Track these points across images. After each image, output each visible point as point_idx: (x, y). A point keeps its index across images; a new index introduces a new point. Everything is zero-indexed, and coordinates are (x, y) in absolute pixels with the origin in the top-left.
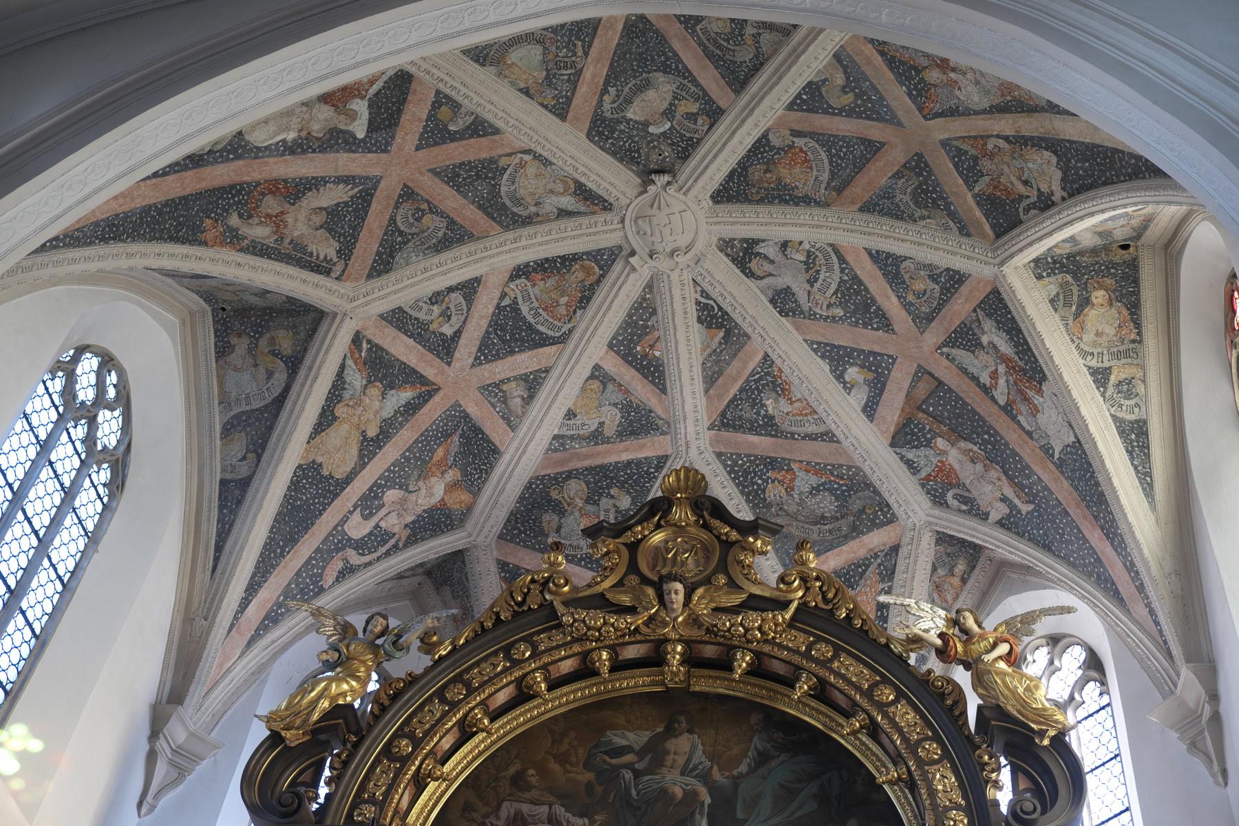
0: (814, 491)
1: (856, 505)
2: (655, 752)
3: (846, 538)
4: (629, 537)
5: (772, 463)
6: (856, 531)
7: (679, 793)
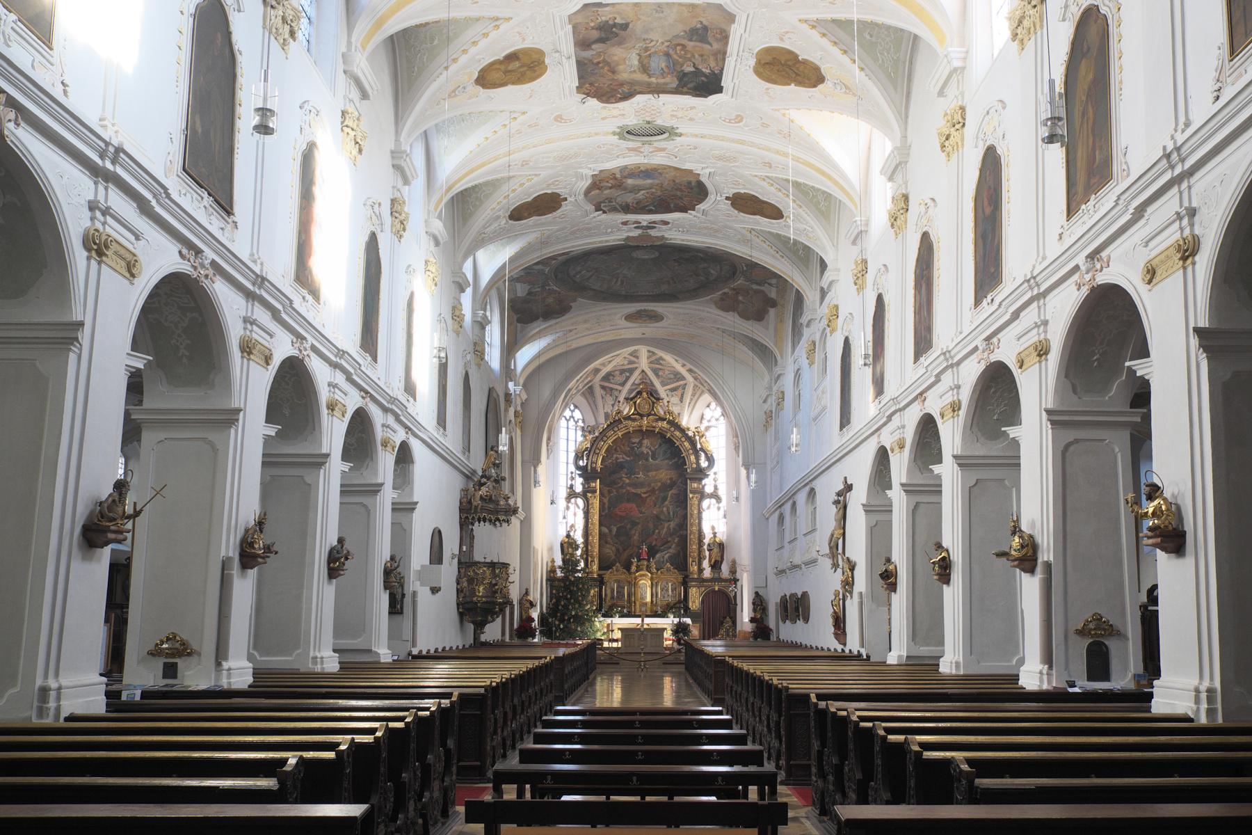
0: (669, 374)
1: (678, 377)
2: (640, 443)
3: (676, 382)
4: (634, 401)
5: (661, 369)
6: (677, 381)
7: (645, 452)
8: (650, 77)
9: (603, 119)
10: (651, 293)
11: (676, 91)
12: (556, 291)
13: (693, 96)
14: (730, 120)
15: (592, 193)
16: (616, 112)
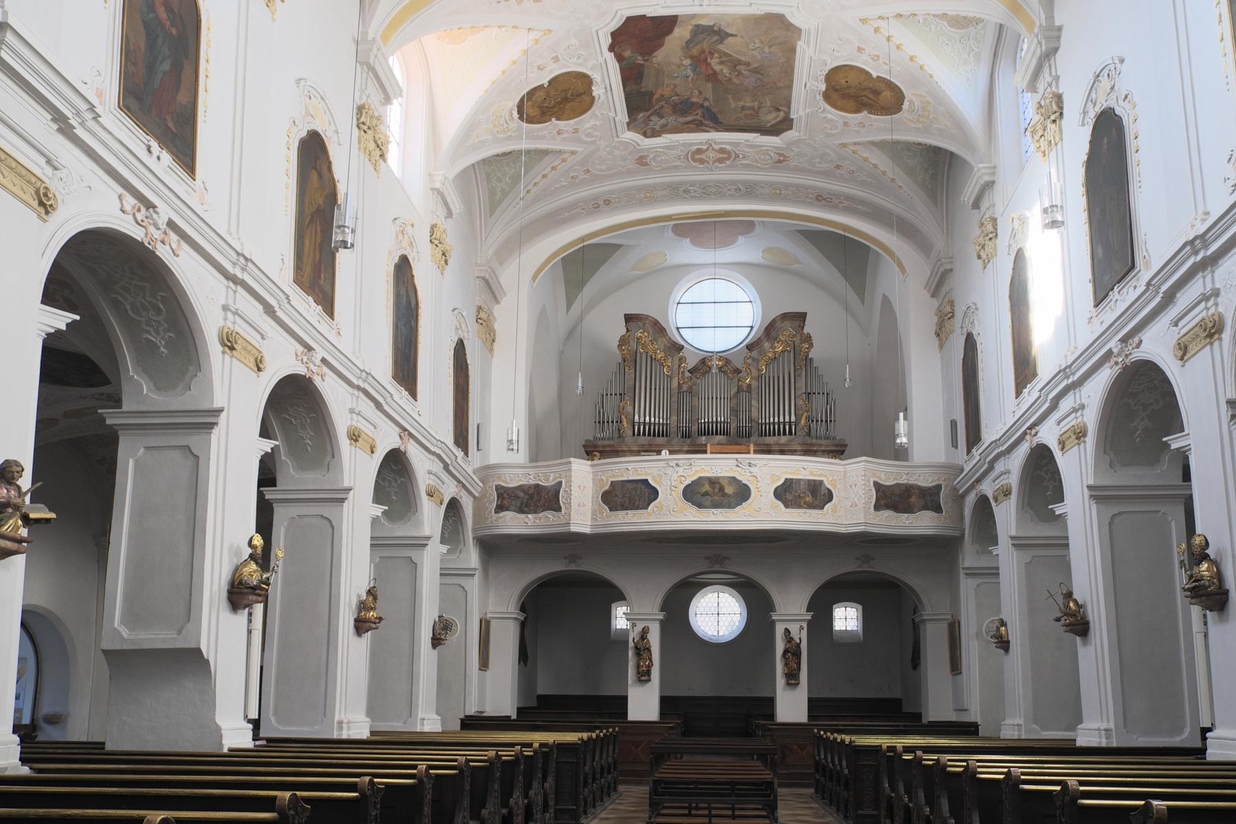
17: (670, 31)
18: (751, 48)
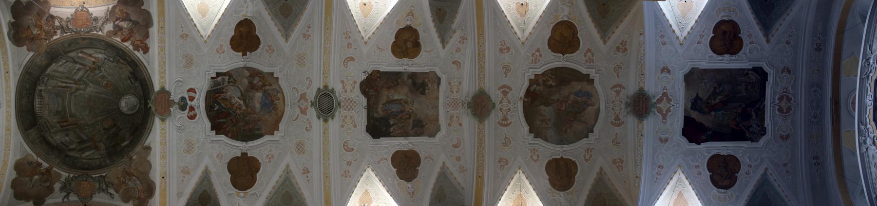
8: (382, 104)
9: (342, 82)
10: (37, 109)
11: (369, 117)
12: (52, 36)
13: (366, 126)
14: (347, 146)
15: (246, 71)
16: (348, 88)
17: (694, 119)
18: (705, 87)
